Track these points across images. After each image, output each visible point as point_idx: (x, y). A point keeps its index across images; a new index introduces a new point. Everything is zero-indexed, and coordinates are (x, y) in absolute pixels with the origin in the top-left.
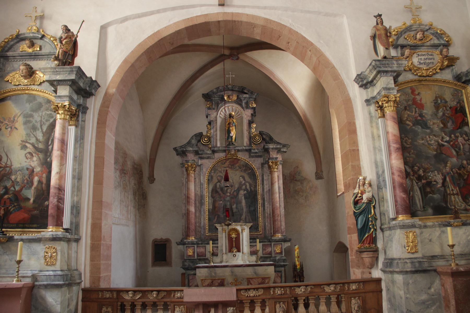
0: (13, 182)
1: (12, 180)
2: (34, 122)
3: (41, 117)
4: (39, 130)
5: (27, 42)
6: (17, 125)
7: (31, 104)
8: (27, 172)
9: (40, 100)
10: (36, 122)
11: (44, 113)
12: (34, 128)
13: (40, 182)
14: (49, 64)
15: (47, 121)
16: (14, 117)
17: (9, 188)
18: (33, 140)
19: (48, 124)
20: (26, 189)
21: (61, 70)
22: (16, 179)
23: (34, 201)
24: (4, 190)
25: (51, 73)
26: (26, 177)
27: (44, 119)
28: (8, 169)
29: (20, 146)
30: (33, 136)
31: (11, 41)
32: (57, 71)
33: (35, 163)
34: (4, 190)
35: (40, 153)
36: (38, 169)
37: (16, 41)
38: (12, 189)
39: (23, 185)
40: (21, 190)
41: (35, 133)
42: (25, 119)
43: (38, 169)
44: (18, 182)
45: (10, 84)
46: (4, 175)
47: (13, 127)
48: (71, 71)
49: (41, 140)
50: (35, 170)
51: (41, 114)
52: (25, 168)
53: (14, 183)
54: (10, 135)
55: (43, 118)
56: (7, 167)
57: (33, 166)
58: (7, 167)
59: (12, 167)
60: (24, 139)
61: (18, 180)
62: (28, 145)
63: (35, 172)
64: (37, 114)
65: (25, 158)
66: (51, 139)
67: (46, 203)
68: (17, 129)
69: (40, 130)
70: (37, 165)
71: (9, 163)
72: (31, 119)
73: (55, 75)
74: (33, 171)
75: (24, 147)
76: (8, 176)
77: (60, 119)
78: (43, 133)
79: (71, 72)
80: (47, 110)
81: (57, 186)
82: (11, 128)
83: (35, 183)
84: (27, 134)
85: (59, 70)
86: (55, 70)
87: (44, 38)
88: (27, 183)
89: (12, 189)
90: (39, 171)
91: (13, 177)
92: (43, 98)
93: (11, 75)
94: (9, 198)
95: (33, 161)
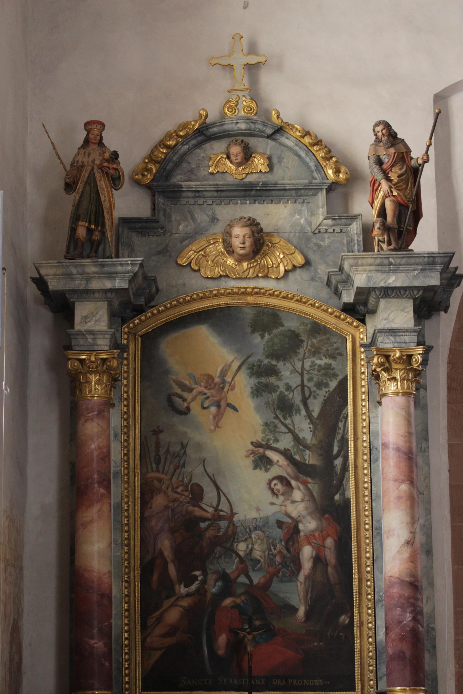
0: (242, 560)
1: (238, 555)
2: (282, 388)
3: (302, 375)
4: (298, 411)
5: (236, 150)
6: (231, 398)
7: (267, 336)
8: (278, 533)
9: (291, 324)
10: (289, 388)
11: (307, 364)
12: (285, 407)
13: (318, 560)
14: (300, 213)
15: (319, 385)
16: (223, 374)
17: (233, 576)
18: (286, 442)
19: (322, 394)
20: (281, 581)
21: (404, 261)
22: (251, 550)
23: (309, 615)
24: (220, 584)
25: (373, 268)
26: (278, 546)
27: (310, 380)
28: (223, 524)
29: (251, 458)
30: (283, 429)
31: (183, 145)
32: (390, 264)
33: (298, 505)
34: (220, 584)
35: (309, 480)
36: (309, 525)
37: (194, 142)
38: (243, 579)
39: (271, 569)
40: (266, 585)
41: (288, 422)
42: (253, 381)
43: (309, 525)
44: (259, 561)
45: (193, 274)
46: (217, 541)
47: (223, 403)
48: (428, 264)
49: (309, 442)
50: (301, 526)
51: (299, 365)
52: (272, 521)
53: (247, 563)
54: (217, 426)
55: (306, 377)
56: (221, 518)
57: (294, 514)
58: (221, 518)
59: (235, 519)
60: (259, 437)
61: (257, 554)
62: (274, 456)
63: (302, 534)
64: (288, 364)
65: (269, 493)
66: (338, 437)
67: (344, 619)
68: (235, 409)
69: (303, 412)
70: (304, 513)
71: (224, 506)
72: (272, 380)
73: (382, 272)
74: (296, 531)
75: (262, 462)
76: (228, 545)
77: (396, 394)
78: (312, 422)
79: (428, 267)
80: (316, 352)
81: (407, 579)
82: (219, 406)
83: (307, 565)
84: (266, 424)
85: (398, 261)
86: (386, 262)
87: (278, 136)
88: (284, 564)
89: (243, 579)
90: (313, 531)
91: (242, 547)
92: (300, 317)
93: (194, 247)
94: (235, 606)
95: (294, 502)
